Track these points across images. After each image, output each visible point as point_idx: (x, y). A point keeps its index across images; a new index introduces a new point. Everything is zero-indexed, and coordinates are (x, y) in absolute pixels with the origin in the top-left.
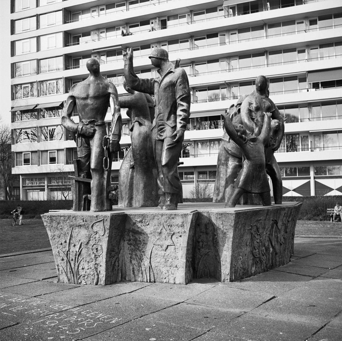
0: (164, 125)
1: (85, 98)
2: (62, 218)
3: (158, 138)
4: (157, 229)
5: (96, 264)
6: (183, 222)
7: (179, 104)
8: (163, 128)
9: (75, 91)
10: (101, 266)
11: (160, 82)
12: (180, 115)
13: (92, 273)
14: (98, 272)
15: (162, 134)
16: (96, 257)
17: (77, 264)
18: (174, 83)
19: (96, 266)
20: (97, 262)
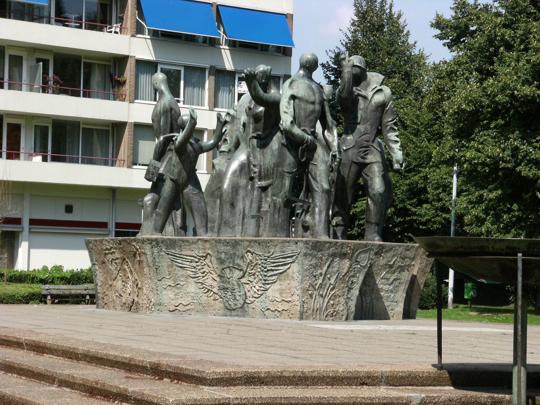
0: (367, 147)
1: (313, 103)
2: (327, 245)
3: (357, 159)
4: (389, 261)
5: (348, 298)
6: (415, 255)
7: (391, 128)
8: (366, 151)
10: (352, 300)
11: (370, 98)
12: (397, 142)
13: (341, 308)
14: (348, 307)
15: (365, 157)
16: (350, 289)
17: (326, 300)
18: (386, 103)
19: (347, 300)
20: (349, 296)
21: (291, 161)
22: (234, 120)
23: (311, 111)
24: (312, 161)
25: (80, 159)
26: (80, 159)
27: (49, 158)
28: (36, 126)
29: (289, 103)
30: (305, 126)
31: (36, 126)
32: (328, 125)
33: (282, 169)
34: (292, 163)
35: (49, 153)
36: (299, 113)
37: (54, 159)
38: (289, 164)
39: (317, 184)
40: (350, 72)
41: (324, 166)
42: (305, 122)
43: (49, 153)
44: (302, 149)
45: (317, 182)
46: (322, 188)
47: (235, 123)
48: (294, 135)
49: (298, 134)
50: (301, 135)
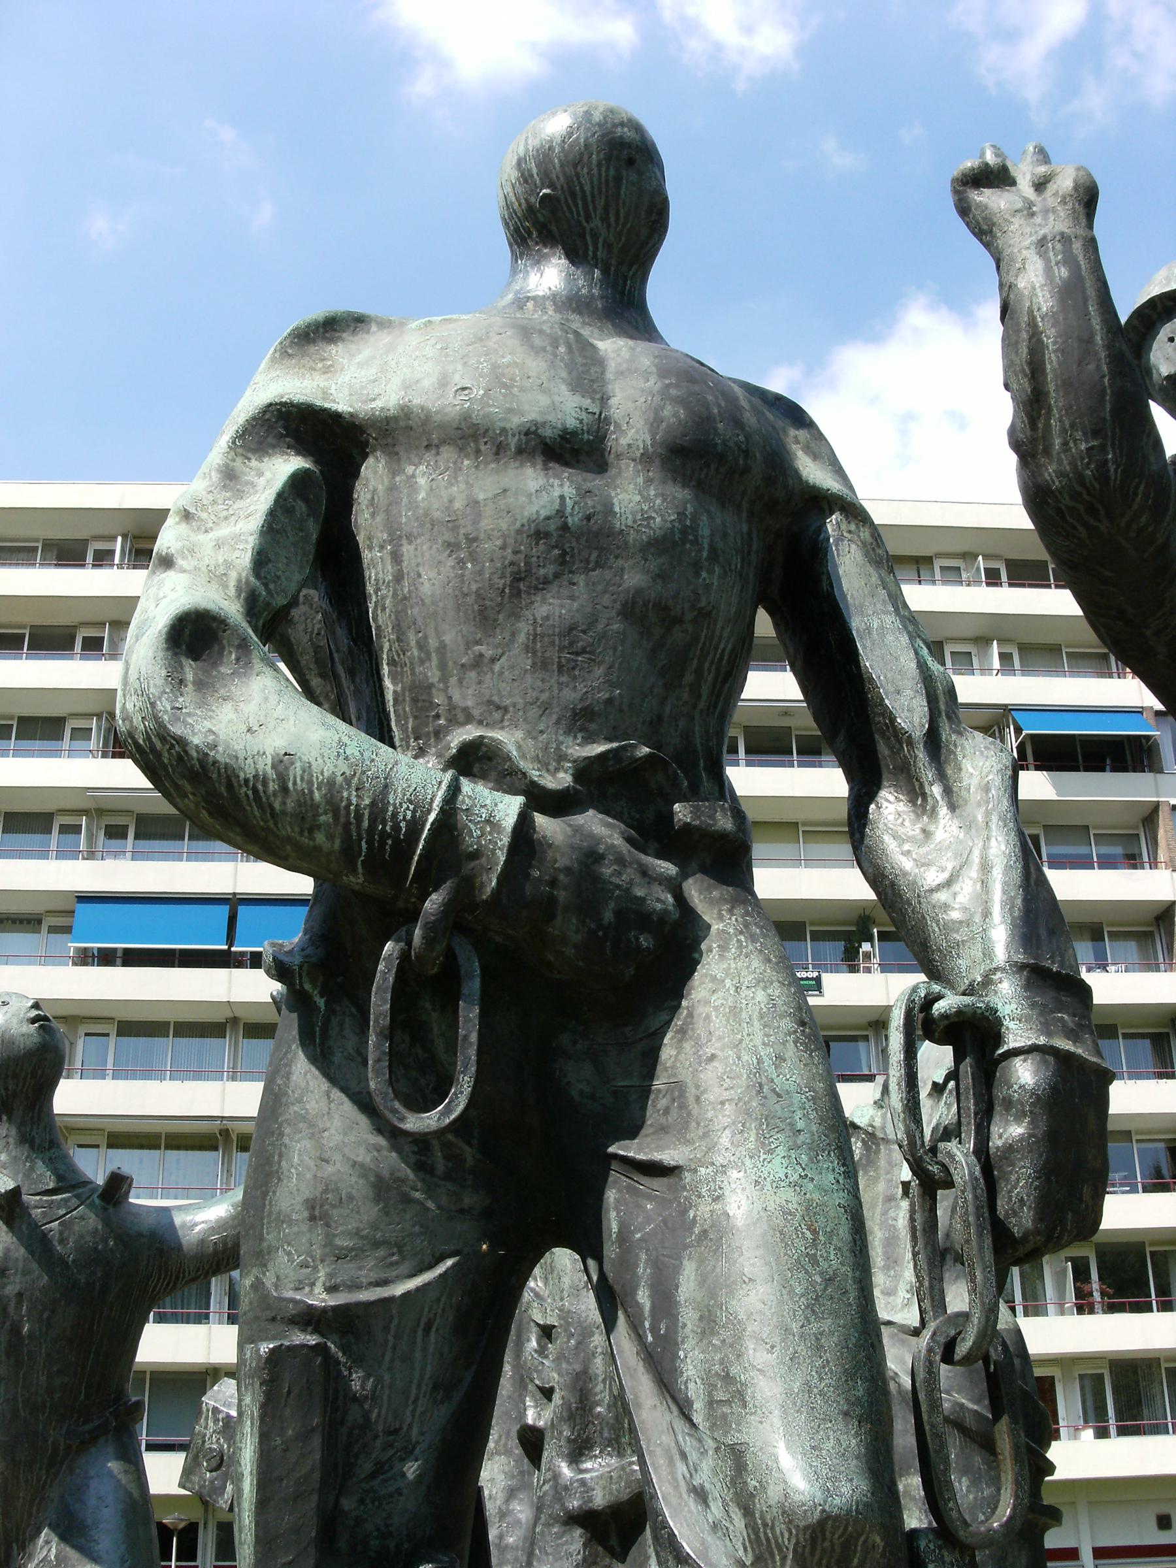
9: (344, 378)
21: (336, 1168)
22: (878, 1152)
23: (539, 534)
24: (632, 1131)
25: (1170, 1424)
26: (1170, 1424)
27: (1113, 1430)
28: (1082, 1377)
29: (229, 477)
30: (496, 711)
31: (1082, 1377)
32: (898, 737)
33: (258, 1285)
34: (357, 1186)
35: (1112, 1421)
36: (399, 577)
37: (1123, 1431)
38: (317, 1212)
39: (688, 1444)
40: (1065, 239)
41: (777, 1167)
42: (478, 662)
43: (1112, 1421)
44: (405, 957)
45: (685, 1412)
46: (745, 1502)
47: (882, 1163)
48: (229, 775)
49: (283, 762)
50: (328, 766)
